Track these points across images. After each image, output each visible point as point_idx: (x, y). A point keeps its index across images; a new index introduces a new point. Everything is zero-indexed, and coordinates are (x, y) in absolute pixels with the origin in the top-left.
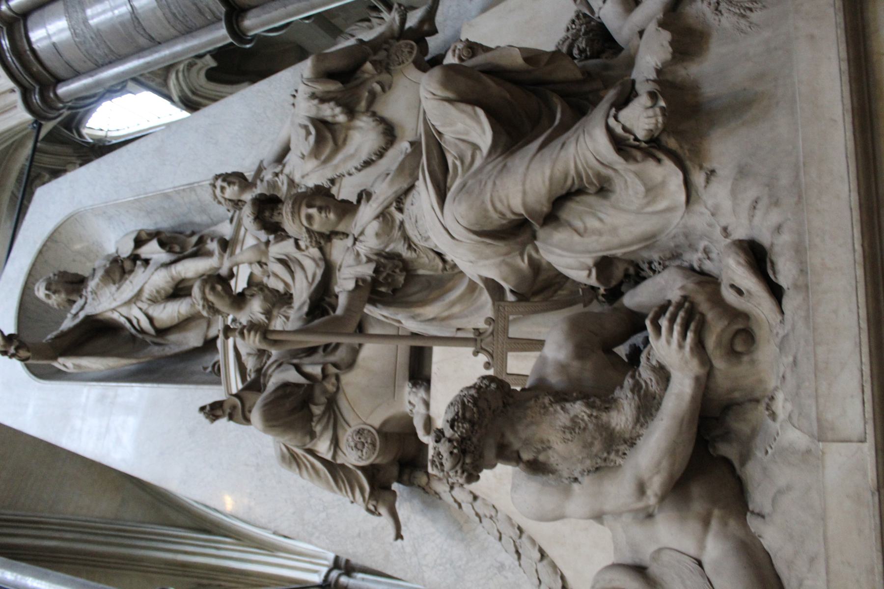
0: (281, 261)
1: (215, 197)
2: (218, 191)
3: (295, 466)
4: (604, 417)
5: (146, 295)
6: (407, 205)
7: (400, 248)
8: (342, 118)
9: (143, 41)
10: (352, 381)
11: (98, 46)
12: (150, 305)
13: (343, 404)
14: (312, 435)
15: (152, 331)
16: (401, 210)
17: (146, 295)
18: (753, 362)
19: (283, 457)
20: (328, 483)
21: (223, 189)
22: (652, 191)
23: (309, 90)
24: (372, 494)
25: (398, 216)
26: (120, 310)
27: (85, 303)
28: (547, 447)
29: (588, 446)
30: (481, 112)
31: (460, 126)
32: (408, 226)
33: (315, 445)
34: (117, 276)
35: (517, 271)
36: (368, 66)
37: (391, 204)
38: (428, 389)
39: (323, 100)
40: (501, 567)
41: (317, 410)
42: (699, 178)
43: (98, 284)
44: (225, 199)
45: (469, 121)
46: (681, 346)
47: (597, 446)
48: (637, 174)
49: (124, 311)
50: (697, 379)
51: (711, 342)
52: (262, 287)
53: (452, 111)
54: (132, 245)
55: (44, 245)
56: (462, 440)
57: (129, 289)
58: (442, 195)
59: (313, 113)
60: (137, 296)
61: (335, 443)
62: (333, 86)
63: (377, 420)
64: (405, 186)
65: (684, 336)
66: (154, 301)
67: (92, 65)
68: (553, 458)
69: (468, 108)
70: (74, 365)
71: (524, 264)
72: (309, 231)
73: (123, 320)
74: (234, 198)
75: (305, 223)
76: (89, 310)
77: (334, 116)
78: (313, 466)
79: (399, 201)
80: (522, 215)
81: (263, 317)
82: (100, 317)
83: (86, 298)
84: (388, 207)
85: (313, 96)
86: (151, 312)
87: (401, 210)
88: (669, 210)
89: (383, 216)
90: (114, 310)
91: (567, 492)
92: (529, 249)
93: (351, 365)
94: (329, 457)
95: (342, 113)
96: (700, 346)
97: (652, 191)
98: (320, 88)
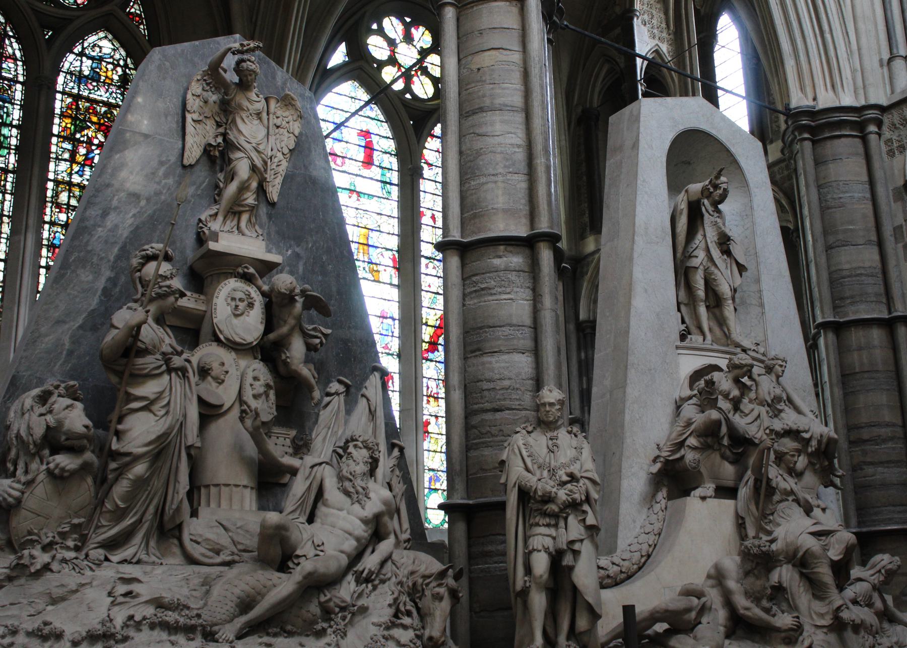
0: (759, 416)
1: (777, 359)
2: (780, 362)
3: (685, 424)
4: (765, 598)
5: (713, 269)
6: (795, 505)
7: (776, 498)
8: (810, 450)
9: (831, 239)
10: (716, 457)
11: (834, 199)
12: (704, 266)
13: (710, 451)
14: (698, 436)
15: (688, 264)
16: (793, 500)
17: (713, 269)
18: (781, 644)
19: (690, 419)
20: (675, 440)
21: (781, 366)
22: (822, 616)
23: (824, 435)
24: (667, 460)
25: (790, 498)
26: (703, 241)
27: (710, 214)
28: (757, 578)
29: (759, 592)
30: (841, 556)
31: (837, 546)
32: (787, 503)
33: (694, 437)
34: (722, 241)
35: (779, 554)
36: (826, 463)
37: (795, 496)
38: (715, 497)
39: (819, 442)
40: (634, 521)
41: (709, 440)
42: (825, 630)
43: (720, 228)
44: (775, 365)
45: (839, 552)
46: (792, 624)
47: (758, 595)
48: (827, 613)
49: (703, 245)
50: (780, 628)
51: (791, 633)
52: (743, 395)
53: (843, 546)
54: (741, 261)
55: (732, 155)
56: (769, 554)
57: (716, 253)
58: (813, 534)
59: (815, 436)
60: (710, 258)
61: (694, 448)
62: (823, 446)
63: (703, 470)
64: (801, 504)
65: (795, 625)
66: (706, 270)
67: (822, 182)
68: (751, 579)
69: (844, 552)
70: (682, 210)
71: (781, 558)
72: (787, 453)
73: (697, 242)
74: (774, 370)
75: (792, 453)
76: (706, 215)
77: (811, 447)
78: (684, 433)
79: (797, 501)
80: (812, 569)
81: (731, 396)
82: (699, 222)
83: (712, 216)
84: (795, 496)
85: (821, 436)
86: (701, 267)
87: (793, 500)
88: (812, 618)
89: (792, 492)
90: (705, 236)
91: (738, 582)
92: (786, 561)
93: (723, 457)
94: (688, 443)
95: (812, 451)
96: (791, 629)
97: (822, 616)
98: (825, 440)
